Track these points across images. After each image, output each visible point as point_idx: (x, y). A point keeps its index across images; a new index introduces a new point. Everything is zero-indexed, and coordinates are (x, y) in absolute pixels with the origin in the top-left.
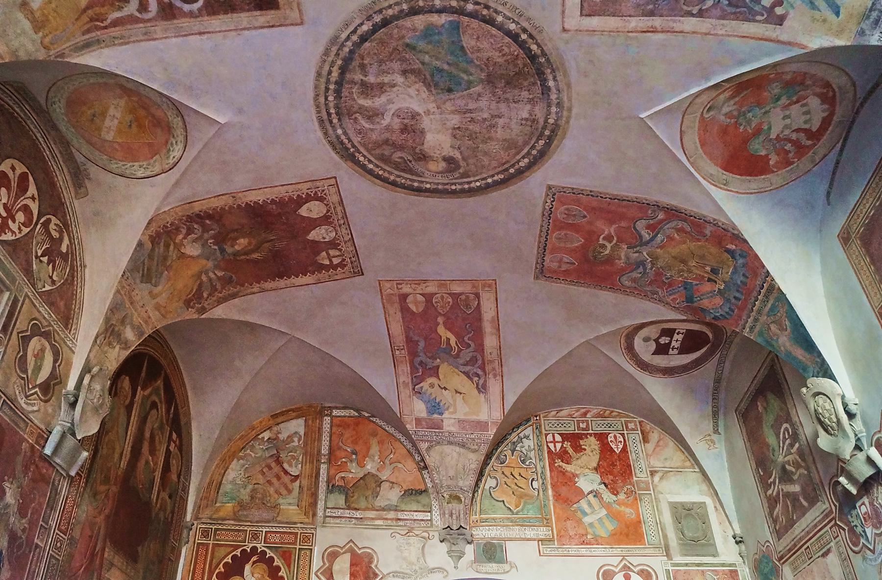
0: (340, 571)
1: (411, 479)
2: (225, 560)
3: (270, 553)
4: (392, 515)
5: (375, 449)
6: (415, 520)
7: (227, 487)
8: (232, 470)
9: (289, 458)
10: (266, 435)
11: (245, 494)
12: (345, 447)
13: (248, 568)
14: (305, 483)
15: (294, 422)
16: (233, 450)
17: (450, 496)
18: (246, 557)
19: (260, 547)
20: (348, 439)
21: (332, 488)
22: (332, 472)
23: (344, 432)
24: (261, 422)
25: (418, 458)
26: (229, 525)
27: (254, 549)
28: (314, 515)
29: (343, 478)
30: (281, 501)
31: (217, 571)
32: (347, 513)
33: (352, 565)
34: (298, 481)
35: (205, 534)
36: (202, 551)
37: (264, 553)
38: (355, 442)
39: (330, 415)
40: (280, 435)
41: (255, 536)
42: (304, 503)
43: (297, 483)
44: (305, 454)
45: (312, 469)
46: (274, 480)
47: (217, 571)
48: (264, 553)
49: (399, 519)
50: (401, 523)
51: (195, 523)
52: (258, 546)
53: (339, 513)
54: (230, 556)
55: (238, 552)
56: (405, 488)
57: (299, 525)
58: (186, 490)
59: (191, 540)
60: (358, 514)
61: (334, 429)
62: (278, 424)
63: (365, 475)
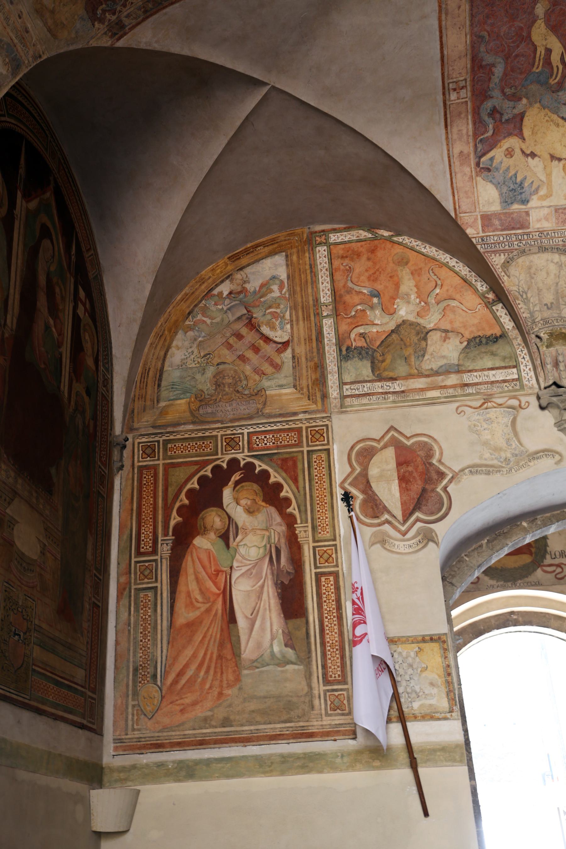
0: (381, 477)
1: (476, 321)
2: (189, 486)
3: (260, 466)
4: (453, 379)
5: (408, 285)
6: (492, 382)
7: (172, 374)
8: (178, 348)
9: (269, 317)
10: (225, 288)
11: (205, 382)
12: (357, 288)
13: (227, 494)
14: (301, 350)
15: (268, 263)
16: (174, 318)
17: (551, 335)
18: (221, 476)
19: (243, 457)
20: (360, 275)
21: (346, 353)
22: (344, 327)
23: (352, 264)
24: (213, 270)
25: (482, 287)
26: (186, 431)
27: (234, 463)
28: (325, 396)
29: (362, 335)
30: (266, 383)
31: (178, 505)
32: (378, 387)
33: (399, 464)
34: (289, 351)
35: (149, 451)
36: (148, 477)
37: (250, 466)
38: (373, 278)
39: (326, 243)
40: (247, 286)
41: (232, 443)
42: (304, 383)
43: (288, 354)
44: (294, 308)
45: (310, 329)
46: (250, 354)
47: (178, 505)
48: (250, 466)
49: (467, 385)
50: (470, 390)
51: (130, 437)
52: (239, 456)
53: (366, 388)
54: (195, 479)
55: (207, 471)
56: (468, 335)
57: (301, 416)
58: (108, 383)
59: (127, 463)
60: (397, 386)
61: (336, 263)
62: (241, 269)
63: (398, 326)
